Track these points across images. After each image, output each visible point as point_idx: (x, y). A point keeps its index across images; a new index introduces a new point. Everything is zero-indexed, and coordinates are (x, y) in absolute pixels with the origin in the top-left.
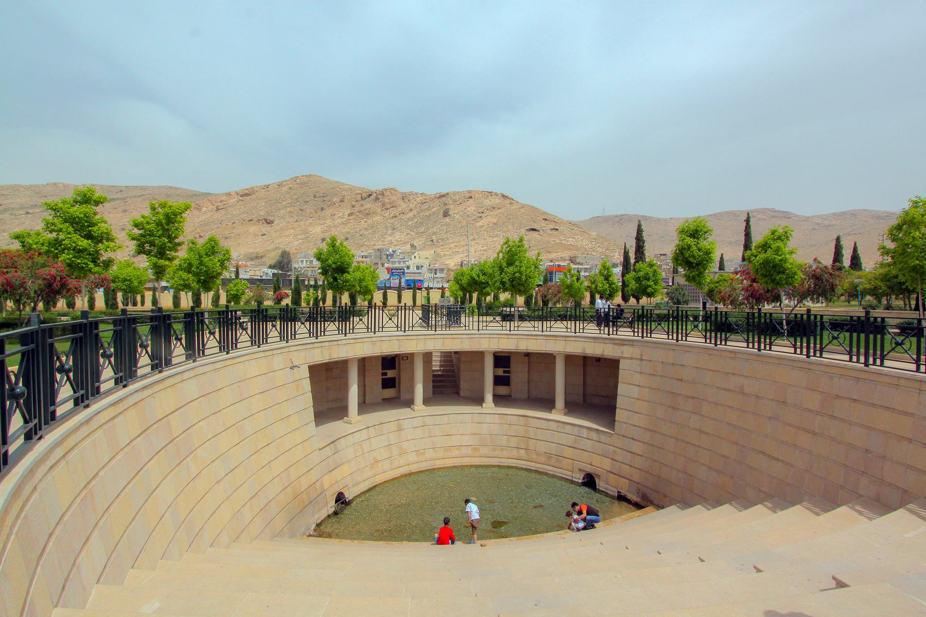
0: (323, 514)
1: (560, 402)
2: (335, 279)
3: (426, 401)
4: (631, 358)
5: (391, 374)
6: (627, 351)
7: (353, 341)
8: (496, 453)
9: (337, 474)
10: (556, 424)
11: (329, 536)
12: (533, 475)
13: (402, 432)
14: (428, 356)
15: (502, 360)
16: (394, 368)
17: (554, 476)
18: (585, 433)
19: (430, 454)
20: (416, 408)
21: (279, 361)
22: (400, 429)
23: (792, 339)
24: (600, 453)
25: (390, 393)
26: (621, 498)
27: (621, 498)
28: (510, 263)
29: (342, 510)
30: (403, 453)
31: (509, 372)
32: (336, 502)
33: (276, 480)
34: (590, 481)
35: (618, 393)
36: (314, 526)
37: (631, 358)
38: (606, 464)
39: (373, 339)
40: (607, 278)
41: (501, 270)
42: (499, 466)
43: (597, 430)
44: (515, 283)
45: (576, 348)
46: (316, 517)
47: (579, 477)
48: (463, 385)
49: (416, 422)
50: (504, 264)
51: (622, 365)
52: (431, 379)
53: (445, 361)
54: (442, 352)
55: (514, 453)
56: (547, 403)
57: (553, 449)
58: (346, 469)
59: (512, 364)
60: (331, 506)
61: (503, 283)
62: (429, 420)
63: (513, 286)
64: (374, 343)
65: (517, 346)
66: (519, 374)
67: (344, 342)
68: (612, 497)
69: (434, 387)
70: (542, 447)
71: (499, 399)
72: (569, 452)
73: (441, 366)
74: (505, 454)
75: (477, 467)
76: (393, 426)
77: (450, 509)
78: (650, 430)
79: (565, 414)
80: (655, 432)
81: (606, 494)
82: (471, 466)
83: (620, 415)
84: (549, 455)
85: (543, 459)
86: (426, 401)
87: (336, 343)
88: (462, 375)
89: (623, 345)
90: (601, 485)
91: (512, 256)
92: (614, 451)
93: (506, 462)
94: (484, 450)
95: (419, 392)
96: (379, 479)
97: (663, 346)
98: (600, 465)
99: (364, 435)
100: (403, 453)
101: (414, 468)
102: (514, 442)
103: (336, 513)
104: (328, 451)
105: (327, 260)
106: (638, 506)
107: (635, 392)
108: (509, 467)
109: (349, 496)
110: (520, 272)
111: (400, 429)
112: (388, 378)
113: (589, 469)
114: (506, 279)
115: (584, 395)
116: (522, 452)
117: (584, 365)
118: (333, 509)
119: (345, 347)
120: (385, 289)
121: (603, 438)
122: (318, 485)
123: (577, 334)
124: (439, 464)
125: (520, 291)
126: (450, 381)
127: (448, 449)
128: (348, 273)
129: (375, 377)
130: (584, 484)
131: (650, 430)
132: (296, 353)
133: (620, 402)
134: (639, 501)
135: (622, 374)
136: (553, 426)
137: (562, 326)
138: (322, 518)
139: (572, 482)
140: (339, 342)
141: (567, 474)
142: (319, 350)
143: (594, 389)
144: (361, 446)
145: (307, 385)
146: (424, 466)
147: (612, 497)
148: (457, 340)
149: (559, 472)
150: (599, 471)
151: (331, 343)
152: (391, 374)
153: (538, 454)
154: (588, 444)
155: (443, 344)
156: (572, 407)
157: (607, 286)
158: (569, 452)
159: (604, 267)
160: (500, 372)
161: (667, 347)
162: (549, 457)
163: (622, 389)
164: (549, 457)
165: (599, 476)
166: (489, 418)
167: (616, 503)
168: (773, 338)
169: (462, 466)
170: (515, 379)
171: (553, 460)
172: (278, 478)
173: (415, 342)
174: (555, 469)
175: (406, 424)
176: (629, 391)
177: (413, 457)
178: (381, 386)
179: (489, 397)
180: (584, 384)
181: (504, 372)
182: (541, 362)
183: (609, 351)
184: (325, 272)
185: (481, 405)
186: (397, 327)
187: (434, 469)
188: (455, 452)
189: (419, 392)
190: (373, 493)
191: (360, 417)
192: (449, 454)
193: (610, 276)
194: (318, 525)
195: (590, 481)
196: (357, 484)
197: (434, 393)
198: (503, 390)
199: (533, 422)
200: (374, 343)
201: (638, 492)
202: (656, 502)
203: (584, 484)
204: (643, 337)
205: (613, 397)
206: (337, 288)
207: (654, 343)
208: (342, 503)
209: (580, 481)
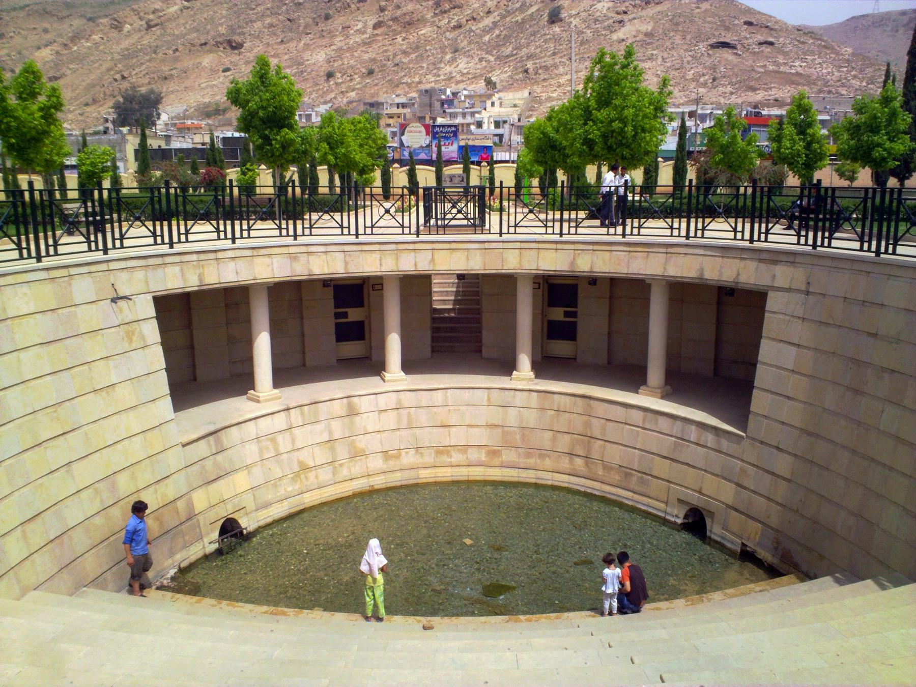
0: (195, 552)
1: (656, 373)
2: (267, 140)
3: (408, 366)
4: (789, 290)
5: (354, 315)
6: (782, 275)
7: (249, 253)
8: (532, 461)
9: (223, 488)
10: (641, 414)
11: (195, 591)
12: (596, 505)
13: (357, 419)
14: (416, 285)
15: (558, 291)
16: (362, 305)
17: (632, 510)
18: (693, 433)
19: (409, 459)
20: (387, 376)
21: (83, 288)
22: (352, 413)
23: (732, 221)
24: (718, 472)
25: (351, 349)
26: (747, 556)
27: (747, 556)
28: (604, 101)
29: (231, 550)
30: (357, 454)
31: (574, 314)
32: (220, 535)
33: (84, 495)
34: (696, 522)
35: (760, 358)
36: (172, 572)
37: (789, 290)
38: (727, 493)
39: (292, 250)
40: (803, 128)
41: (588, 116)
42: (536, 486)
43: (715, 429)
44: (611, 141)
45: (683, 268)
46: (178, 557)
47: (677, 515)
48: (488, 337)
49: (383, 401)
50: (593, 103)
51: (774, 302)
52: (428, 324)
53: (465, 293)
54: (461, 277)
55: (565, 463)
56: (631, 375)
57: (635, 459)
58: (241, 482)
59: (579, 303)
60: (210, 542)
61: (589, 143)
62: (408, 399)
63: (610, 148)
64: (293, 257)
65: (573, 263)
66: (592, 319)
67: (230, 254)
68: (731, 553)
69: (434, 340)
70: (614, 455)
71: (545, 366)
72: (661, 467)
73: (456, 302)
74: (548, 463)
75: (495, 484)
76: (338, 408)
77: (420, 557)
78: (809, 434)
79: (663, 397)
80: (817, 436)
81: (720, 546)
82: (486, 483)
83: (760, 402)
84: (626, 471)
85: (616, 477)
86: (408, 366)
87: (212, 256)
88: (486, 318)
89: (776, 262)
90: (715, 530)
91: (611, 83)
92: (743, 470)
93: (548, 478)
94: (509, 456)
95: (394, 345)
96: (310, 499)
97: (848, 266)
98: (717, 493)
99: (280, 421)
100: (357, 454)
101: (379, 482)
102: (564, 443)
103: (219, 552)
104: (202, 449)
105: (248, 101)
106: (773, 572)
107: (789, 356)
108: (554, 488)
109: (247, 523)
110: (623, 121)
111: (352, 413)
112: (337, 327)
113: (695, 499)
114: (595, 133)
115: (717, 360)
116: (579, 462)
117: (719, 303)
118: (216, 546)
119: (232, 264)
120: (411, 163)
121: (725, 444)
122: (181, 505)
123: (692, 241)
124: (426, 475)
125: (623, 158)
126: (461, 331)
127: (441, 451)
128: (290, 127)
129: (322, 320)
130: (685, 527)
131: (809, 434)
132: (124, 275)
133: (763, 376)
134: (778, 560)
135: (772, 323)
136: (637, 416)
137: (726, 226)
138: (193, 558)
139: (665, 522)
140: (220, 255)
141: (656, 507)
142: (177, 269)
143: (715, 350)
144: (273, 440)
145: (151, 331)
146: (396, 479)
147: (731, 553)
148: (459, 254)
149: (643, 503)
150: (714, 506)
151: (202, 257)
152: (354, 315)
153: (607, 468)
154: (696, 455)
155: (432, 260)
156: (678, 384)
157: (800, 146)
158: (661, 467)
159: (799, 106)
160: (558, 314)
161: (857, 266)
162: (627, 475)
163: (767, 351)
164: (627, 475)
165: (712, 514)
166: (520, 399)
167: (737, 565)
168: (770, 225)
169: (468, 482)
170: (576, 326)
171: (634, 479)
172: (90, 490)
173: (377, 256)
174: (636, 497)
175: (364, 404)
176: (780, 356)
177: (376, 463)
178: (333, 337)
179: (524, 361)
180: (718, 342)
181: (567, 314)
182: (626, 292)
183: (746, 274)
184: (246, 124)
185: (510, 374)
186: (342, 227)
187: (417, 485)
188: (456, 457)
189: (394, 345)
190: (297, 521)
191: (276, 391)
192: (445, 459)
193: (810, 125)
194: (183, 571)
195: (696, 522)
196: (267, 505)
197: (434, 350)
198: (561, 348)
199: (601, 409)
200: (293, 257)
201: (776, 547)
202: (804, 568)
203: (685, 527)
204: (814, 246)
205: (752, 365)
206: (277, 159)
207: (833, 258)
208: (235, 536)
209: (679, 521)
